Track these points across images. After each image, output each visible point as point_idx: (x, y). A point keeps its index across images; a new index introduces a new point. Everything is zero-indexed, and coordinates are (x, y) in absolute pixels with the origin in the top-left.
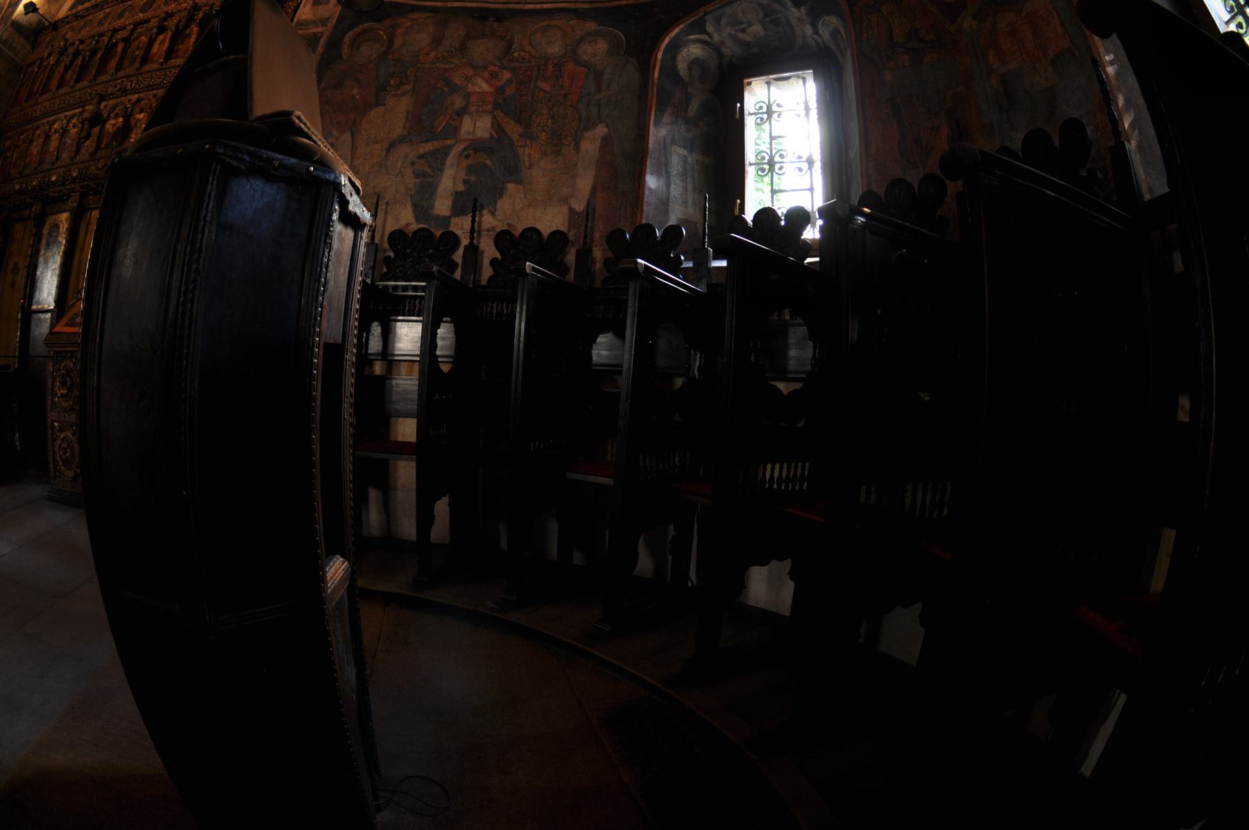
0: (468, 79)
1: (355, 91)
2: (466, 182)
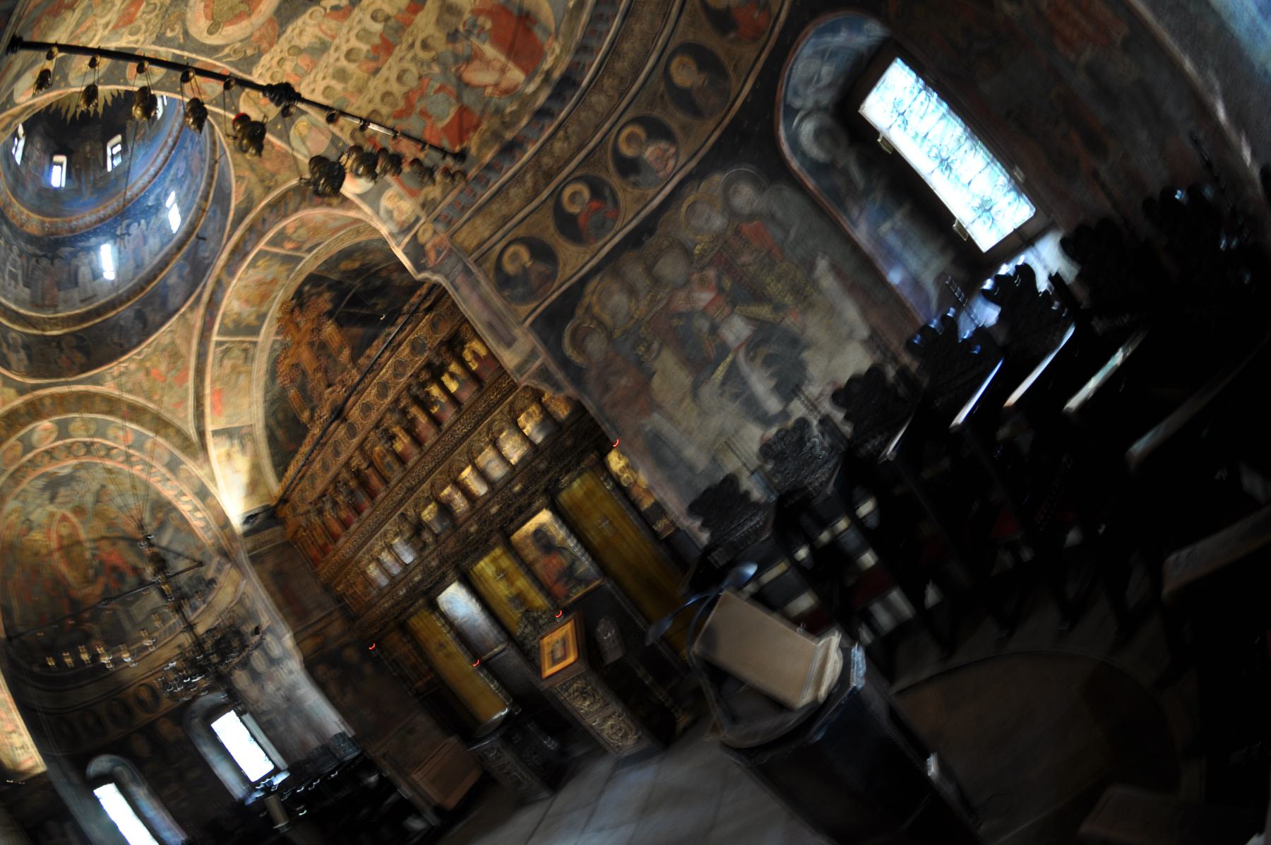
0: (688, 299)
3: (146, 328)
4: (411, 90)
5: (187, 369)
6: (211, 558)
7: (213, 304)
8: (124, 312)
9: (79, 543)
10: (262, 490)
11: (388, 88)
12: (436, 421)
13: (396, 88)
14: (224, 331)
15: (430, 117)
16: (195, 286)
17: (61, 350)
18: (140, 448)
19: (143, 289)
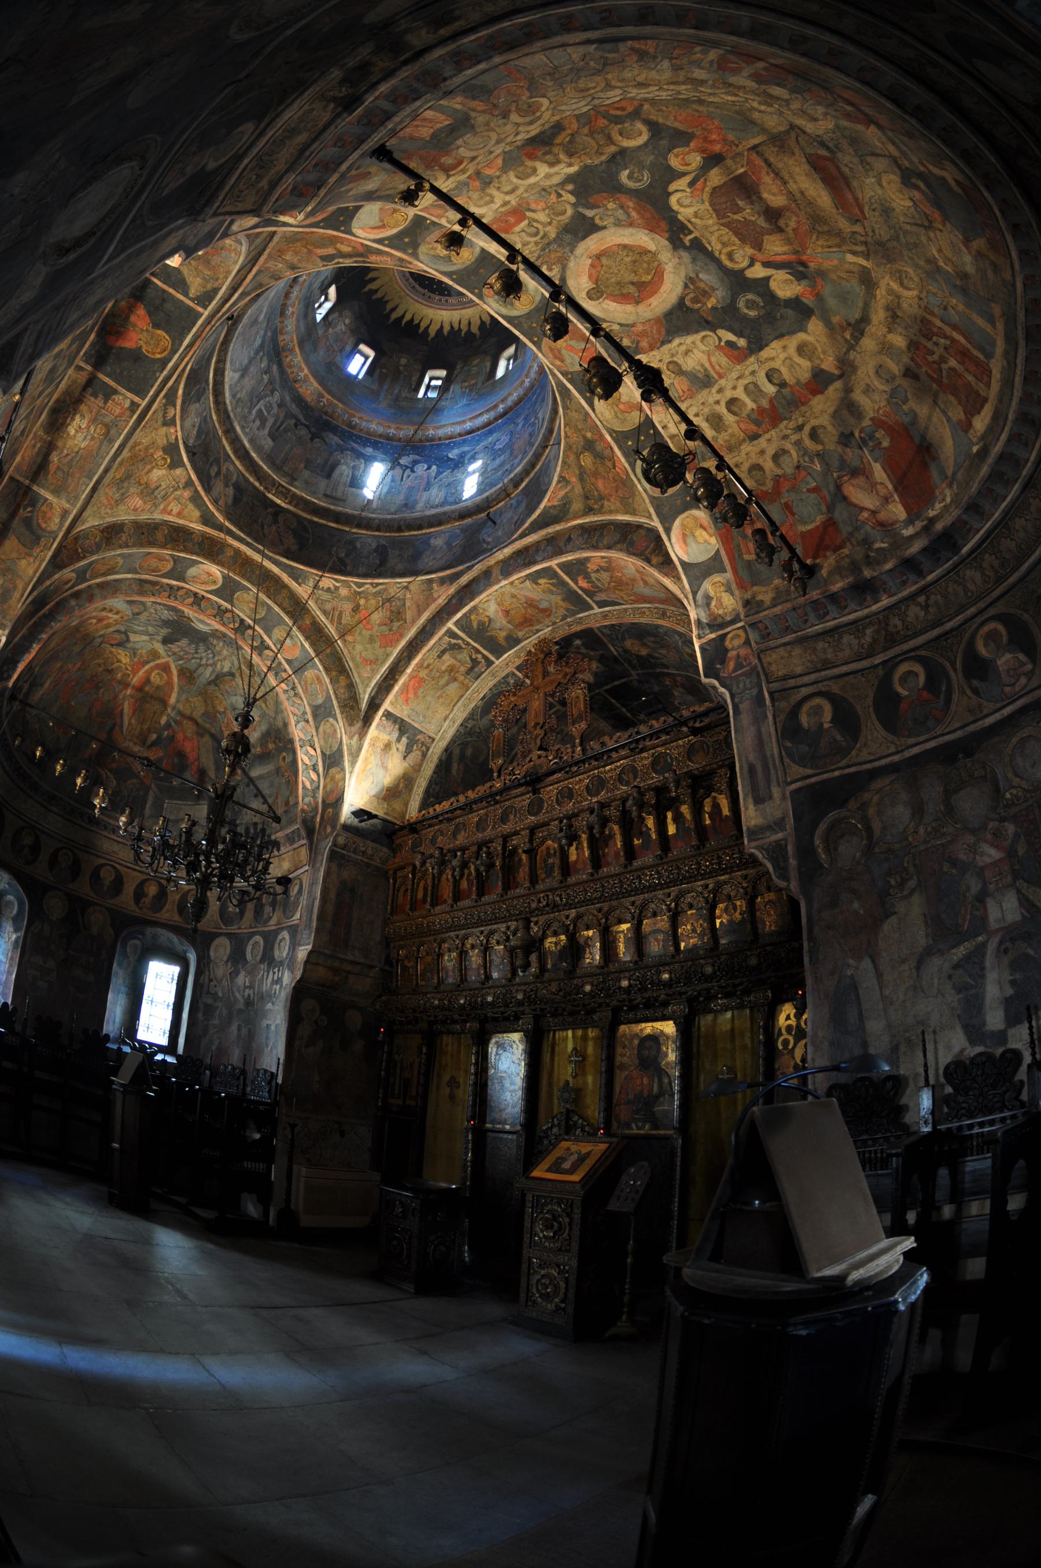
1: (856, 905)
2: (1013, 983)
3: (380, 565)
4: (784, 476)
5: (402, 636)
6: (291, 822)
7: (468, 592)
9: (164, 703)
10: (397, 805)
11: (761, 461)
12: (631, 854)
13: (768, 465)
14: (464, 624)
15: (793, 514)
17: (276, 522)
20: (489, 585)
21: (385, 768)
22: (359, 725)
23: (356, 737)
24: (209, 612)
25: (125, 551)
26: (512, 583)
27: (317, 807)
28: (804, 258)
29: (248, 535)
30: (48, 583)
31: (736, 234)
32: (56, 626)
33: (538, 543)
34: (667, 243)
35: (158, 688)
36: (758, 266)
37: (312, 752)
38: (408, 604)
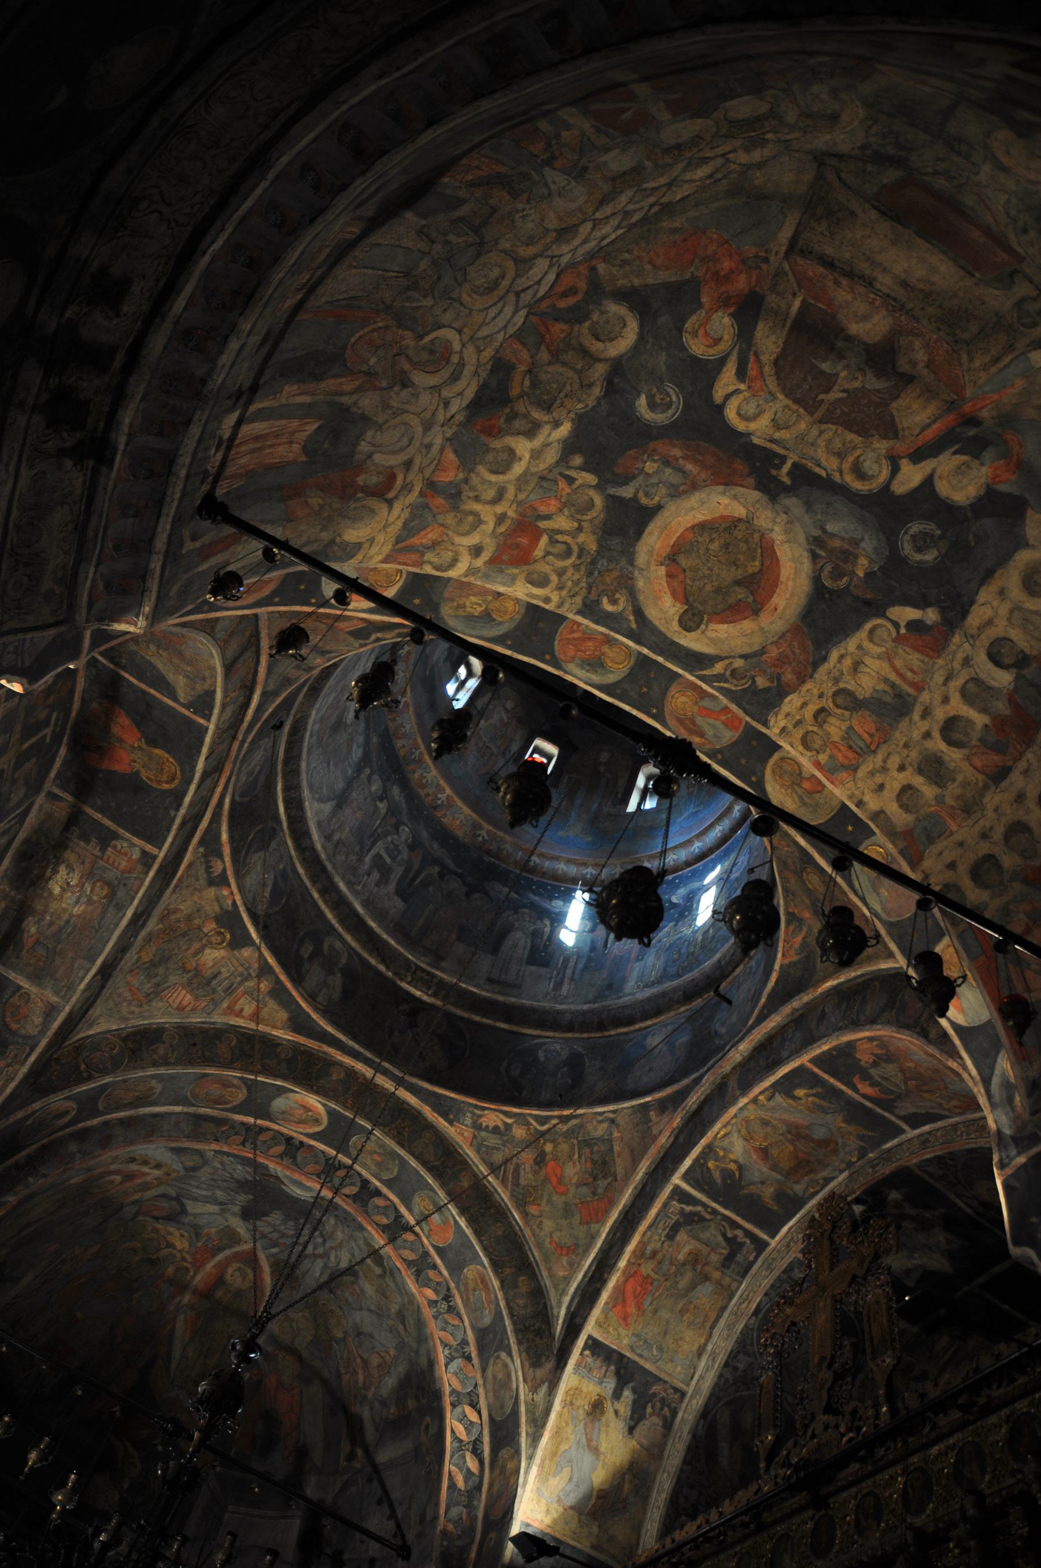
5: (612, 1203)
7: (698, 1122)
8: (554, 1045)
14: (698, 1176)
16: (685, 1072)
18: (456, 1268)
19: (601, 1026)
20: (725, 1108)
21: (595, 1451)
22: (549, 1365)
23: (544, 1389)
24: (310, 1168)
25: (162, 1071)
26: (755, 1100)
27: (472, 1528)
28: (967, 408)
29: (367, 1046)
30: (20, 1115)
31: (849, 426)
32: (35, 1183)
33: (781, 1031)
34: (756, 494)
35: (239, 1293)
36: (905, 465)
37: (473, 1417)
38: (617, 1148)
